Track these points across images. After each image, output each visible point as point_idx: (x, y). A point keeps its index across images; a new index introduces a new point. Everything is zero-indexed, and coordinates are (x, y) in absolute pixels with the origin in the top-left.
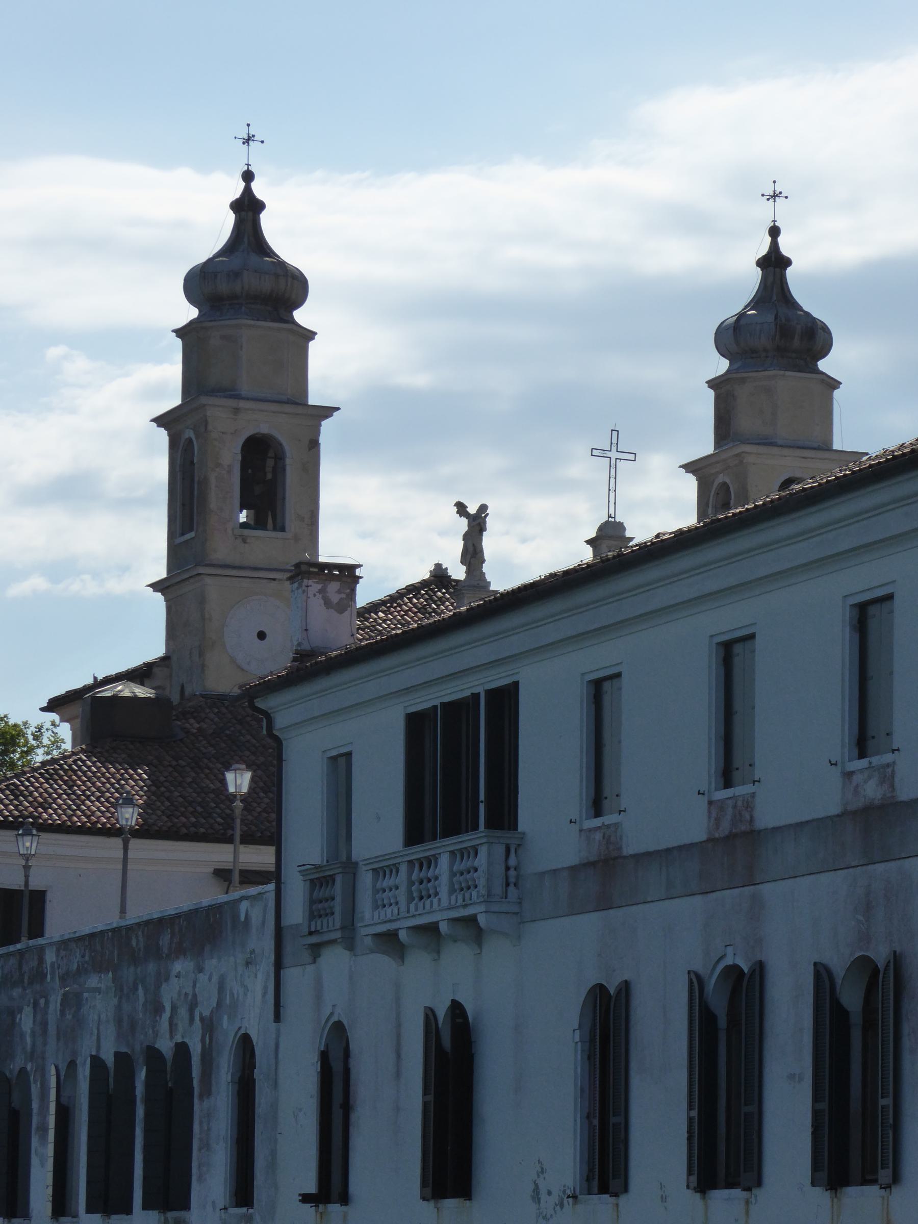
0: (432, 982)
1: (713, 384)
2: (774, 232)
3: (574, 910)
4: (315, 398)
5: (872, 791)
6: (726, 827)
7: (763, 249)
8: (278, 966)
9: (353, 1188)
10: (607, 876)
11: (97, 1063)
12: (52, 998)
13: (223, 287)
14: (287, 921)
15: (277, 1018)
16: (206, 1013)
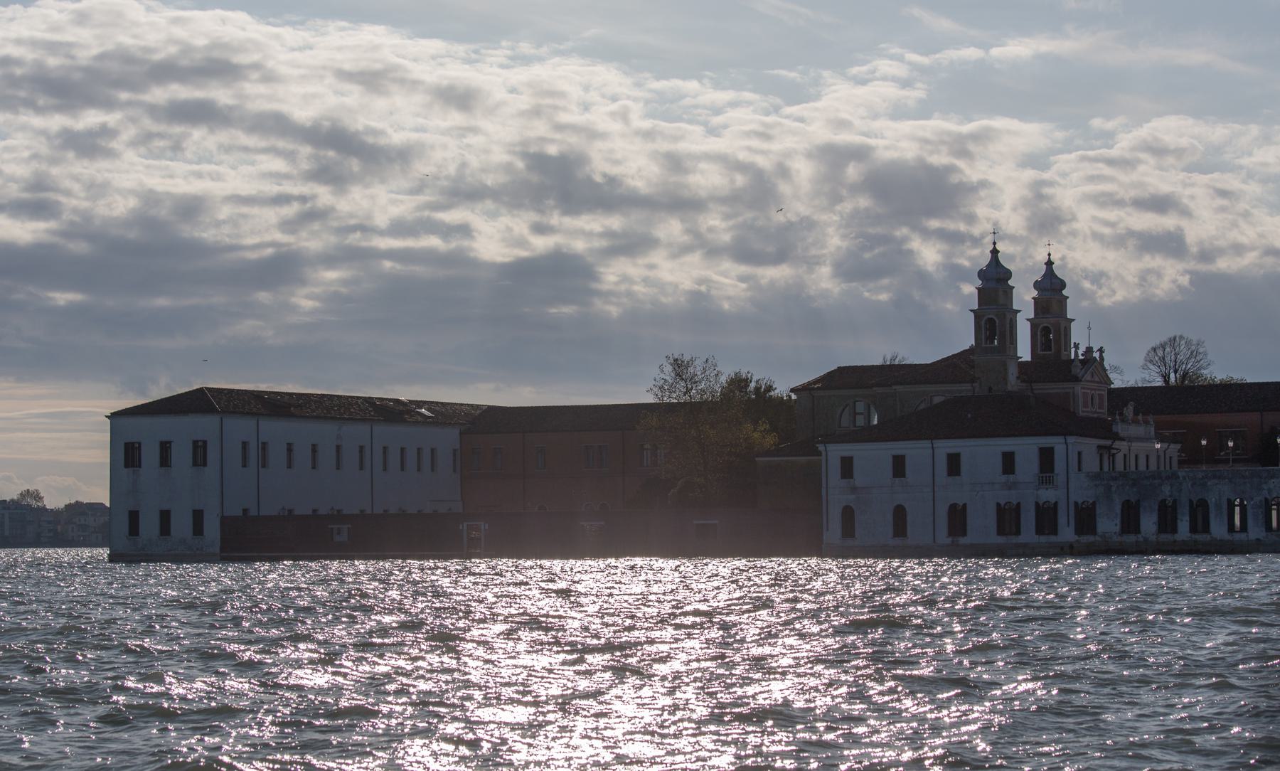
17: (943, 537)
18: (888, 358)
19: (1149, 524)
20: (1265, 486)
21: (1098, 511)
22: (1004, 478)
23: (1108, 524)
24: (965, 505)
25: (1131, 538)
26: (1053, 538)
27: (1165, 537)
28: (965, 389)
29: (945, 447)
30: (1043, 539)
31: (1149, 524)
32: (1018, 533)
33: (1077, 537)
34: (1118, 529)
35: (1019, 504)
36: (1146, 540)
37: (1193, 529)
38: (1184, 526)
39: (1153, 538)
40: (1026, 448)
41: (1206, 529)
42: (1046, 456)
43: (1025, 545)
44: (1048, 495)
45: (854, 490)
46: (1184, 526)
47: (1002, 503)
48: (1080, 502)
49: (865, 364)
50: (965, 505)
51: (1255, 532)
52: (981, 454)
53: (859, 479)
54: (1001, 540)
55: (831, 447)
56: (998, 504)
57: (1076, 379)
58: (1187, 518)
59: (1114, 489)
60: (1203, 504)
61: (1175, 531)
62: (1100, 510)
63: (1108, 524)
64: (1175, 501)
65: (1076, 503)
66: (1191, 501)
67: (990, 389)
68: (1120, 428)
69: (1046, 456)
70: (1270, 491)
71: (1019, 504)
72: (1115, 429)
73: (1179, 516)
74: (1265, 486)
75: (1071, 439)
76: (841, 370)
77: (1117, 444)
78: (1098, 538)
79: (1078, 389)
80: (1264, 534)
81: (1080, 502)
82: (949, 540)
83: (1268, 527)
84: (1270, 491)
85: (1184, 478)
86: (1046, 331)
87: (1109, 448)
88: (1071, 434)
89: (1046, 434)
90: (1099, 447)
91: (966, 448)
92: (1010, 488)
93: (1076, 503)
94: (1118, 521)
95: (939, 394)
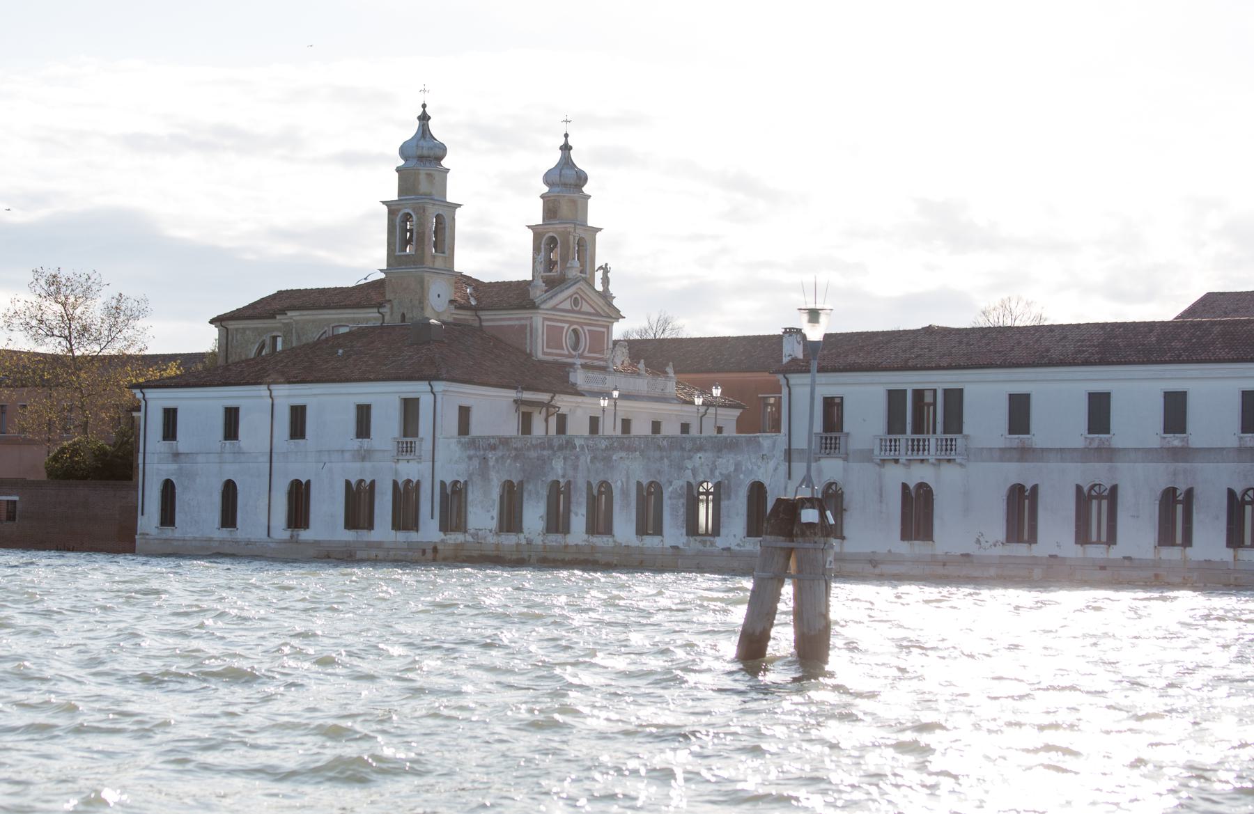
0: (896, 476)
1: (542, 197)
2: (566, 136)
3: (1001, 460)
4: (450, 198)
5: (1177, 443)
6: (1095, 445)
7: (562, 142)
8: (789, 462)
9: (845, 534)
10: (1024, 453)
11: (639, 484)
12: (582, 459)
13: (425, 152)
14: (793, 447)
15: (789, 478)
16: (724, 472)
17: (281, 531)
18: (654, 318)
19: (534, 516)
20: (689, 464)
21: (470, 497)
22: (357, 443)
23: (482, 516)
24: (308, 482)
25: (510, 540)
26: (413, 536)
27: (555, 540)
28: (370, 317)
29: (287, 395)
30: (401, 536)
31: (534, 516)
32: (370, 526)
33: (441, 536)
34: (494, 524)
35: (373, 483)
36: (529, 542)
37: (592, 529)
38: (578, 522)
39: (538, 540)
40: (385, 397)
41: (609, 531)
42: (410, 408)
43: (379, 545)
44: (410, 470)
45: (176, 456)
46: (578, 522)
47: (354, 482)
48: (448, 481)
49: (309, 287)
50: (308, 482)
51: (673, 535)
52: (332, 404)
53: (184, 441)
54: (350, 536)
55: (150, 393)
56: (348, 483)
57: (533, 306)
58: (583, 510)
59: (491, 463)
60: (606, 487)
61: (566, 530)
62: (473, 495)
63: (482, 516)
64: (569, 483)
65: (443, 484)
66: (589, 484)
67: (403, 315)
68: (579, 378)
69: (410, 408)
70: (694, 472)
71: (373, 483)
72: (572, 378)
73: (573, 508)
74: (689, 464)
75: (439, 386)
76: (280, 293)
77: (564, 403)
78: (469, 538)
79: (538, 321)
80: (684, 539)
81: (448, 481)
82: (286, 535)
83: (692, 526)
84: (694, 472)
85: (582, 448)
86: (553, 240)
87: (548, 405)
88: (437, 378)
89: (410, 378)
90: (516, 401)
91: (311, 395)
92: (363, 459)
93: (443, 484)
94: (495, 512)
95: (345, 320)
